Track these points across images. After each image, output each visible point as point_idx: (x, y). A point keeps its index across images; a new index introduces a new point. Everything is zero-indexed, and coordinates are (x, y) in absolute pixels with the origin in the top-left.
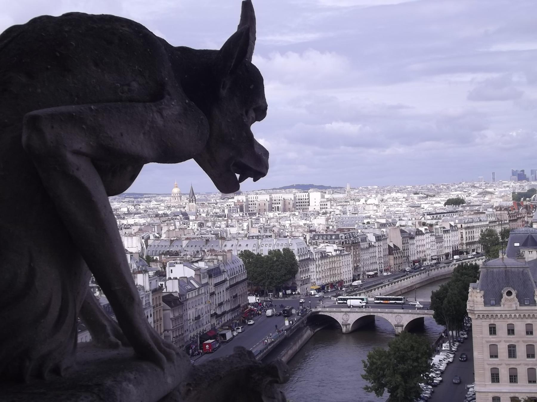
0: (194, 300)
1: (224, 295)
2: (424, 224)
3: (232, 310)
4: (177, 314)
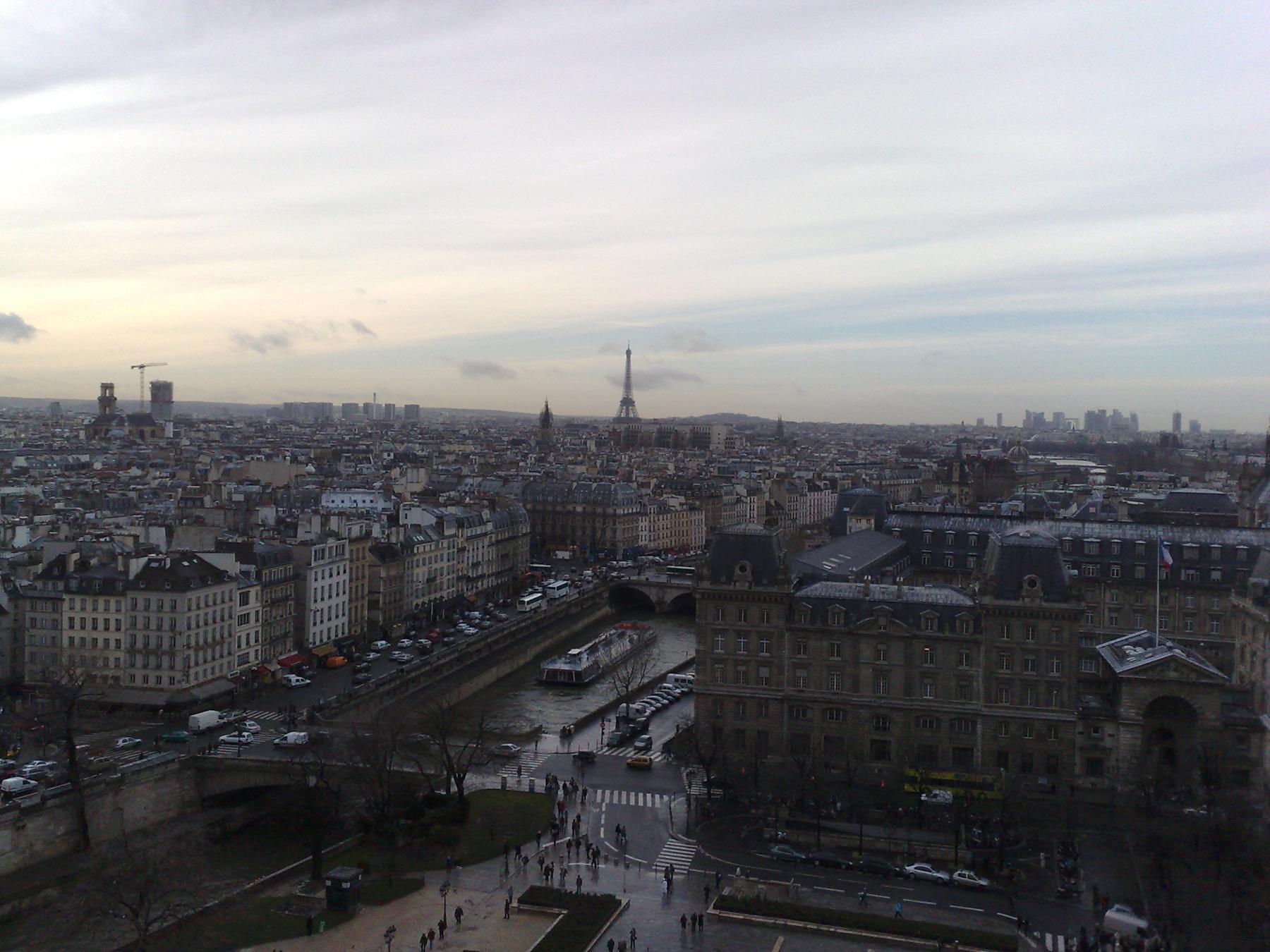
0: (427, 556)
1: (483, 552)
2: (825, 478)
3: (498, 575)
4: (393, 572)
